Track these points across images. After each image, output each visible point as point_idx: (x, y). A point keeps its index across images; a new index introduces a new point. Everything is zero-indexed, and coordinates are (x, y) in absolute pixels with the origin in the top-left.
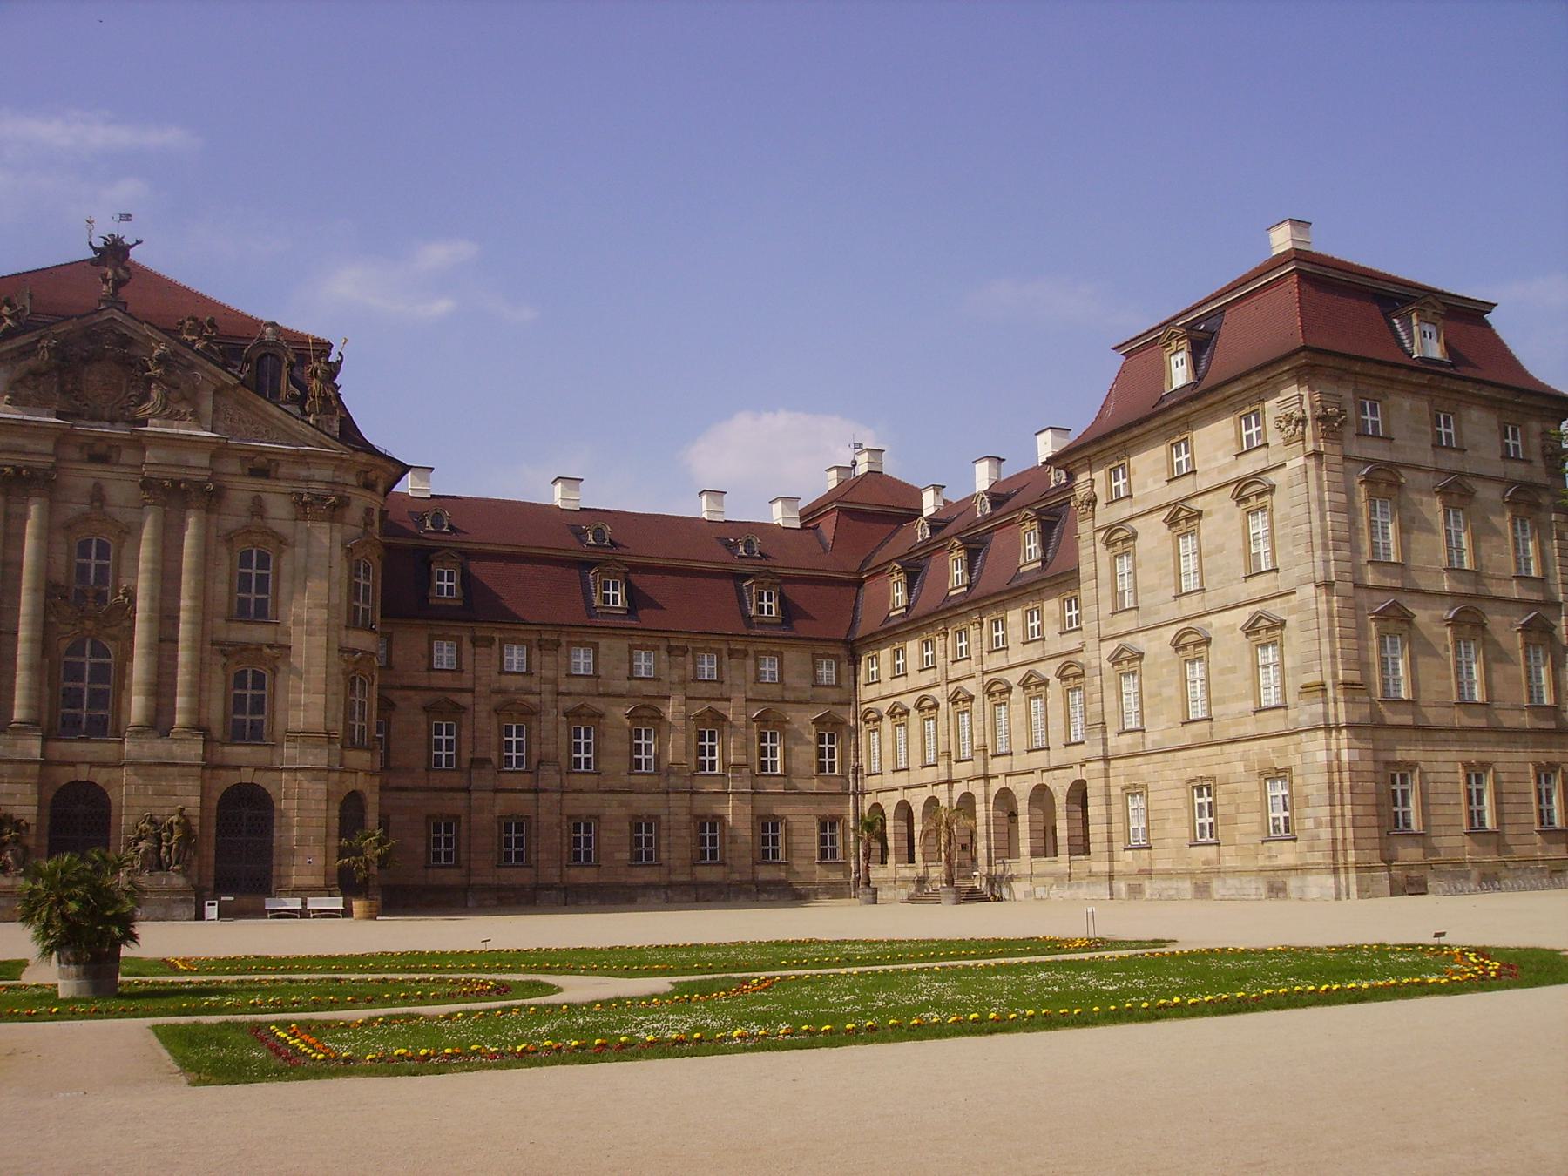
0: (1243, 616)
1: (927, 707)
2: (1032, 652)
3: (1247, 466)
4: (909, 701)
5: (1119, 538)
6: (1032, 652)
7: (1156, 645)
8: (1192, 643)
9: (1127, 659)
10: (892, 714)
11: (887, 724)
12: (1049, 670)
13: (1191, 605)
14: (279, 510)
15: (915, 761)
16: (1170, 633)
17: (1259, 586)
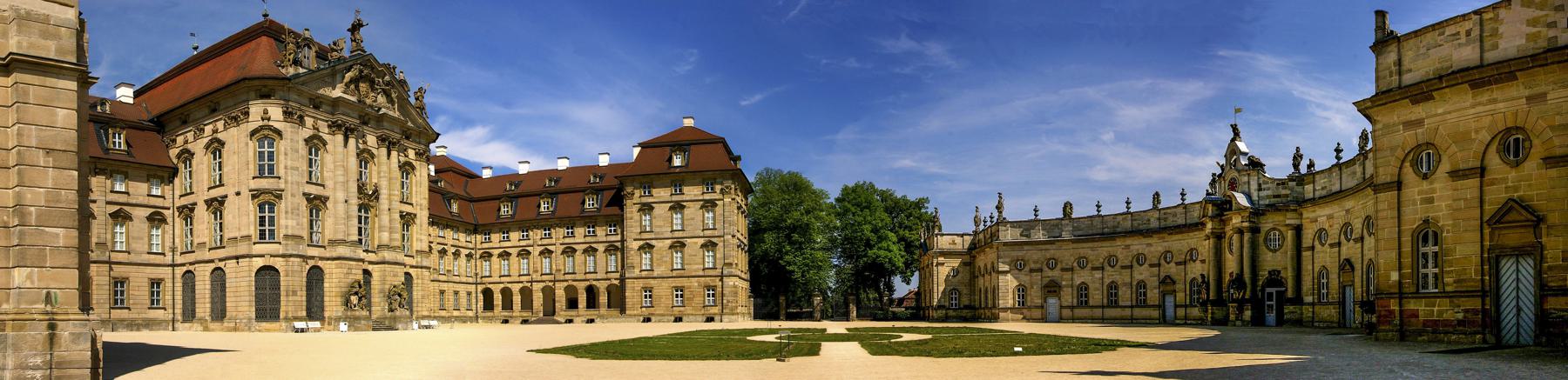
0: (702, 241)
1: (524, 253)
2: (589, 239)
3: (707, 197)
4: (514, 251)
5: (647, 208)
6: (589, 239)
7: (661, 245)
8: (679, 245)
9: (647, 247)
10: (500, 255)
11: (494, 259)
12: (601, 248)
13: (677, 234)
14: (411, 154)
15: (514, 272)
16: (669, 242)
17: (708, 233)
